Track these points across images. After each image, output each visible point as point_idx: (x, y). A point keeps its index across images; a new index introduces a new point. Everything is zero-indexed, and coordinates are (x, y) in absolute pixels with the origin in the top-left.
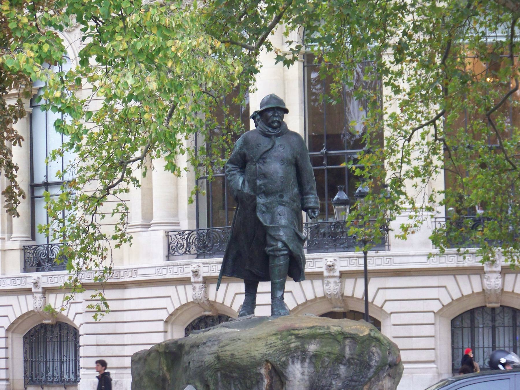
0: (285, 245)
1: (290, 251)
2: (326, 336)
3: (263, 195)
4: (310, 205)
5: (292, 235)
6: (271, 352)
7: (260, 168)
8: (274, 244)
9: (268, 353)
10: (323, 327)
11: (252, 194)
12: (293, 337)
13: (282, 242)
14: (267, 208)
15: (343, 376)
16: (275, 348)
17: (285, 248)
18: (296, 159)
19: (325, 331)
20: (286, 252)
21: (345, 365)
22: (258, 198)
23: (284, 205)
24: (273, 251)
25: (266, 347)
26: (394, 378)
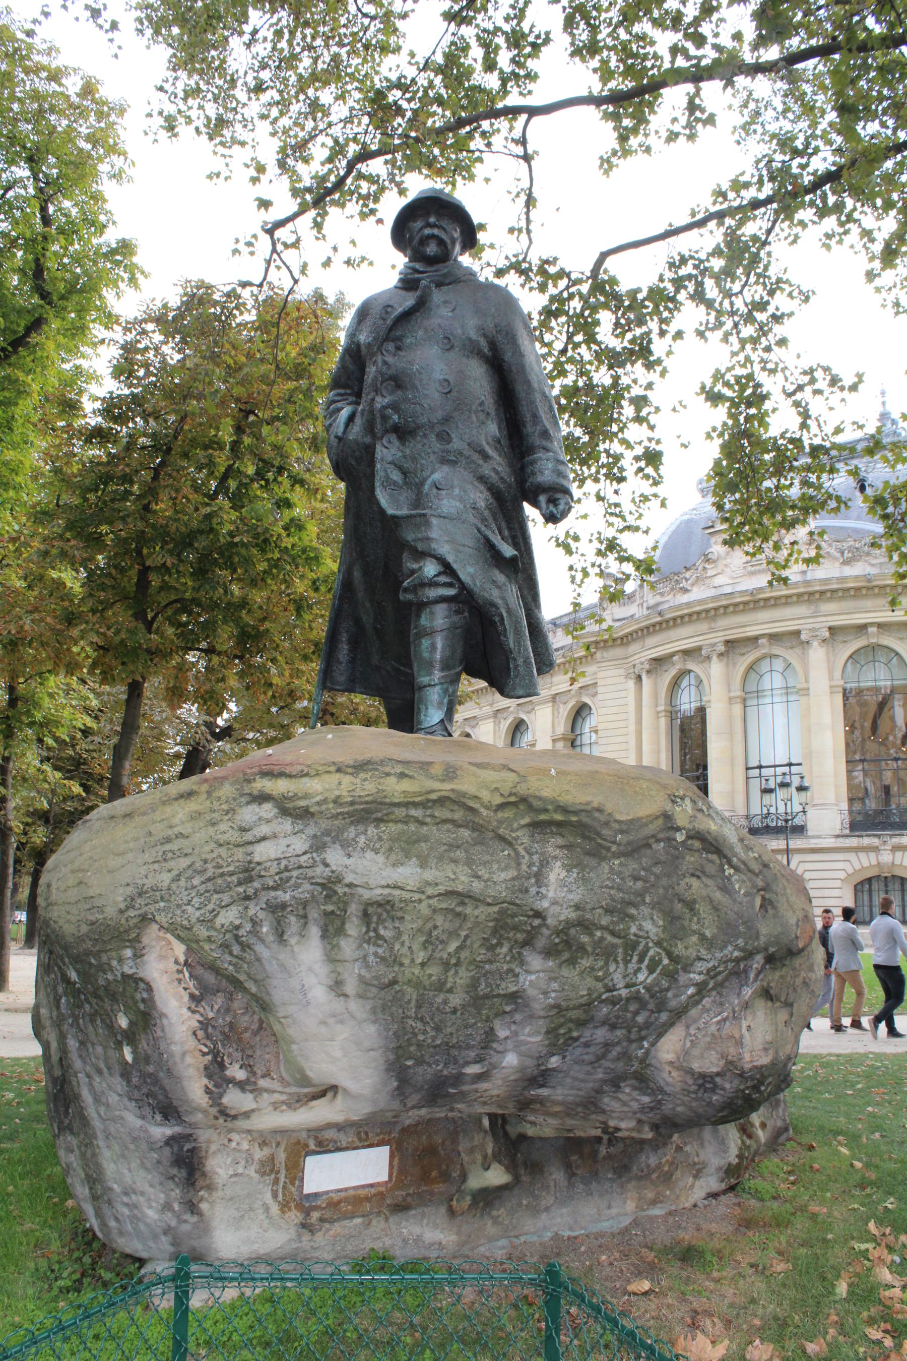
0: (447, 568)
1: (463, 586)
2: (441, 813)
3: (393, 437)
4: (540, 479)
5: (470, 542)
6: (165, 878)
7: (385, 363)
8: (415, 566)
9: (149, 883)
10: (425, 766)
11: (368, 440)
12: (268, 810)
13: (435, 557)
14: (405, 473)
15: (539, 1003)
16: (184, 863)
17: (443, 579)
18: (493, 345)
19: (437, 785)
20: (451, 592)
21: (549, 952)
22: (379, 448)
23: (453, 463)
24: (414, 589)
25: (148, 857)
26: (789, 1005)
